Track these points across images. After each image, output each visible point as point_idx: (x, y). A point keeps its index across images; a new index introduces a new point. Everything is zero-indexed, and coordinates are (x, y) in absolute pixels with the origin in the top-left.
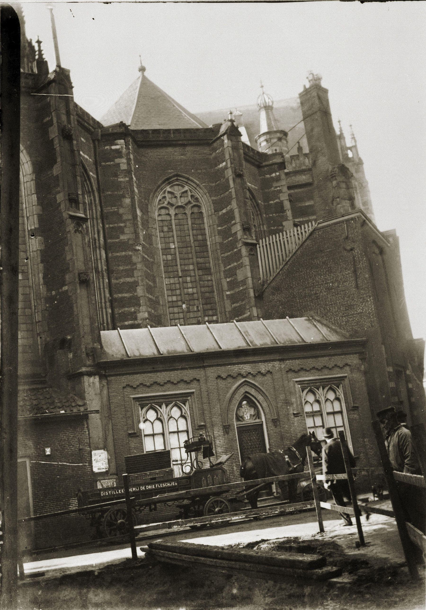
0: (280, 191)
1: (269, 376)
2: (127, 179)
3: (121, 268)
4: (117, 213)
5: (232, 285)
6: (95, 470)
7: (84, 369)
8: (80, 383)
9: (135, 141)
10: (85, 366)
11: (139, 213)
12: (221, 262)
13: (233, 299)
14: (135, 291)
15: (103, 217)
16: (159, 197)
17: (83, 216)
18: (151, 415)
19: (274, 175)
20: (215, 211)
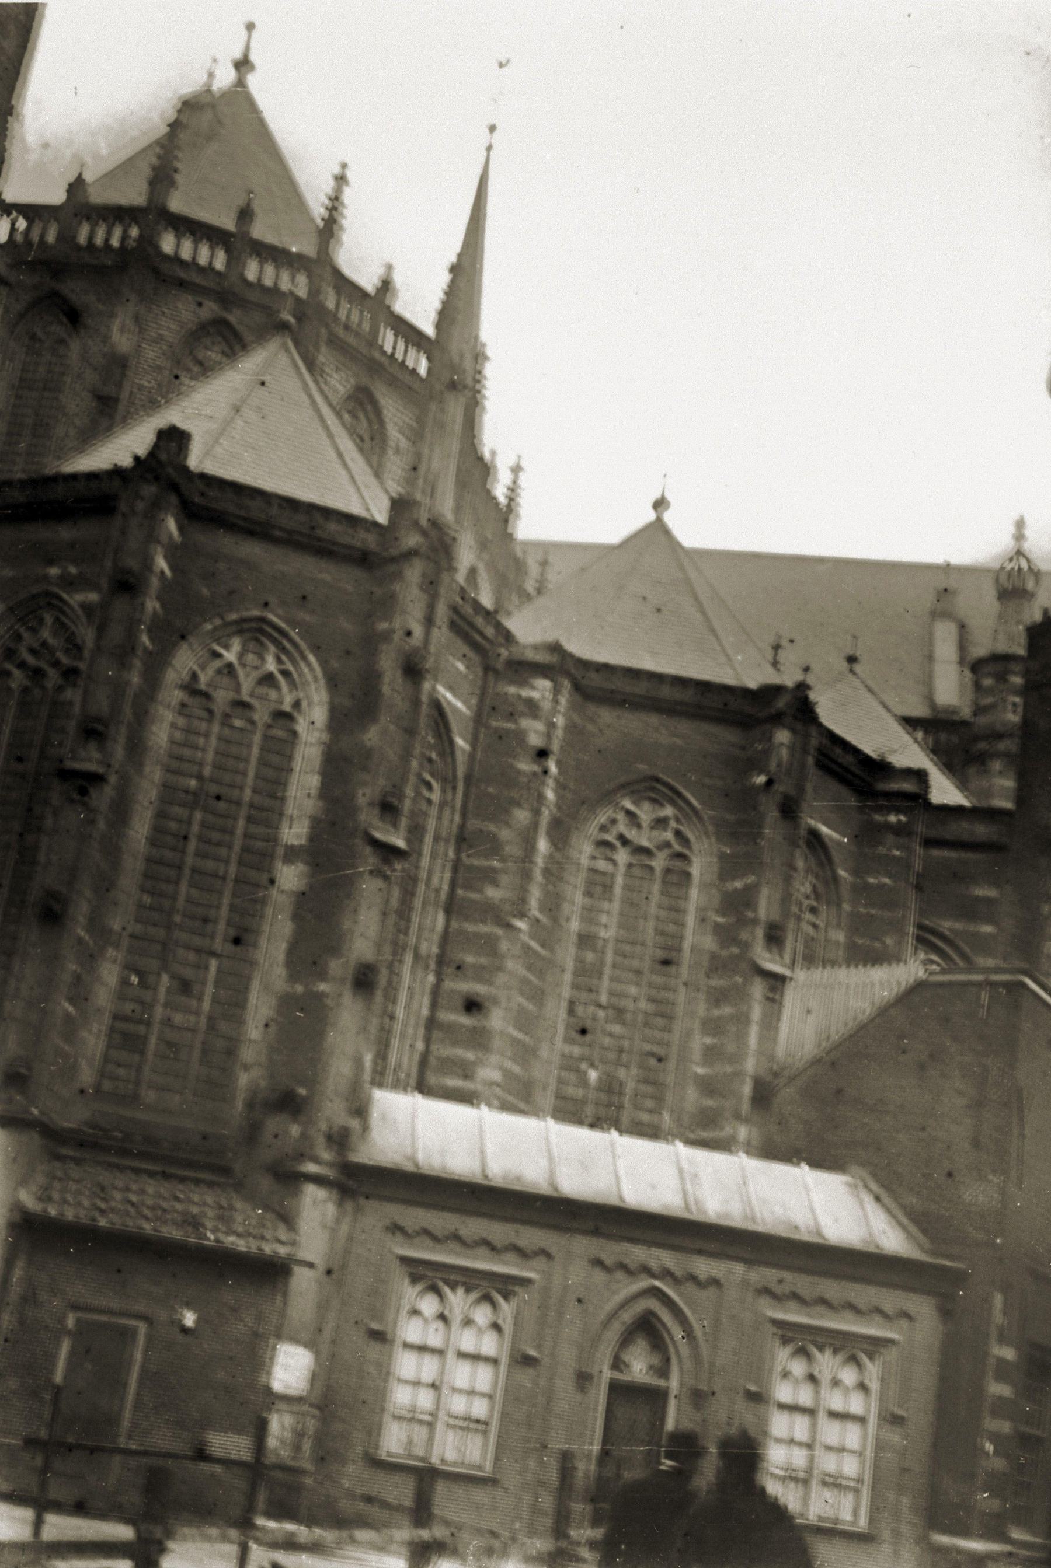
1: (712, 1292)
4: (493, 839)
5: (711, 1054)
6: (277, 1386)
7: (311, 1168)
8: (296, 1193)
9: (577, 687)
10: (316, 1160)
11: (543, 845)
13: (708, 1087)
15: (462, 840)
16: (603, 819)
17: (401, 843)
18: (429, 1305)
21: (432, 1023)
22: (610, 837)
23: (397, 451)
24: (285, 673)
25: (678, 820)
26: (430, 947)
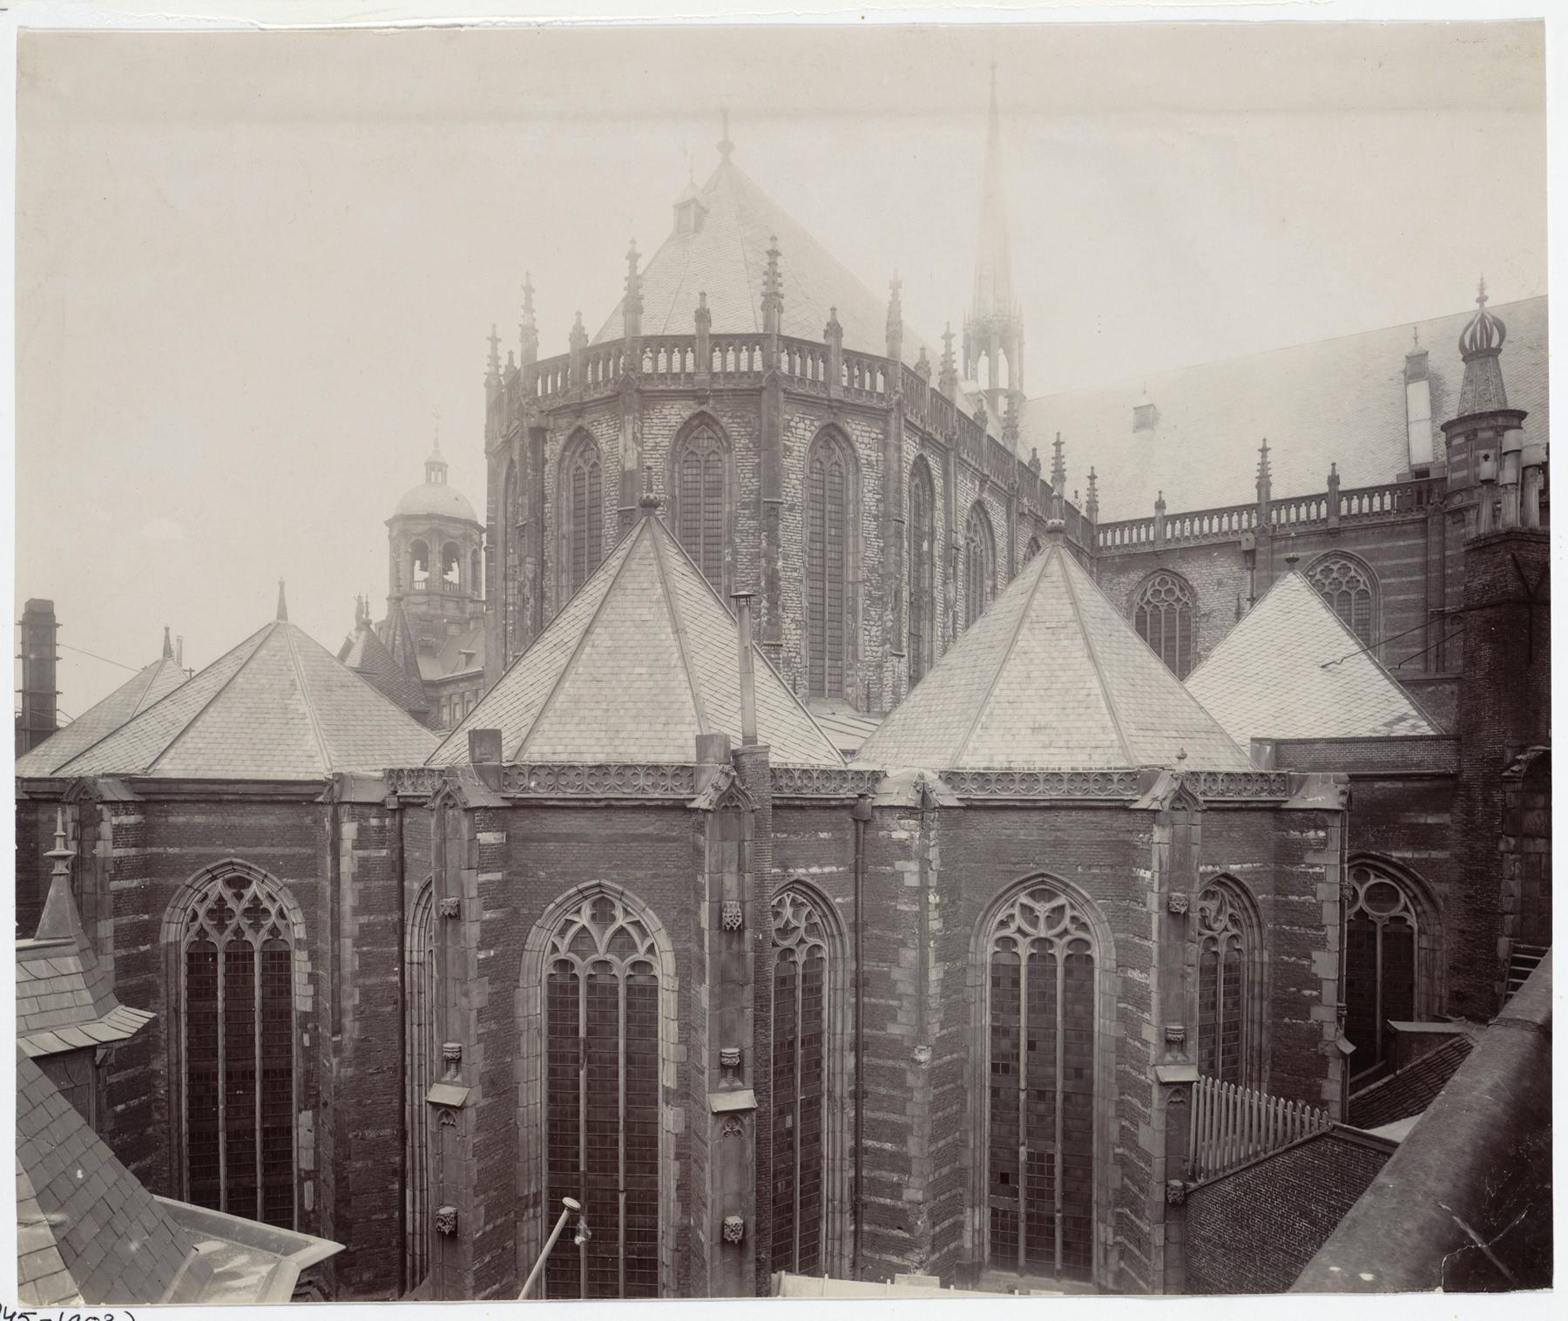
0: (1320, 878)
2: (916, 908)
3: (883, 1091)
4: (885, 976)
12: (1113, 1081)
14: (904, 1142)
16: (1001, 916)
19: (1311, 834)
20: (1118, 966)
21: (857, 1152)
22: (1008, 932)
23: (869, 464)
24: (637, 924)
25: (1073, 907)
26: (844, 1087)
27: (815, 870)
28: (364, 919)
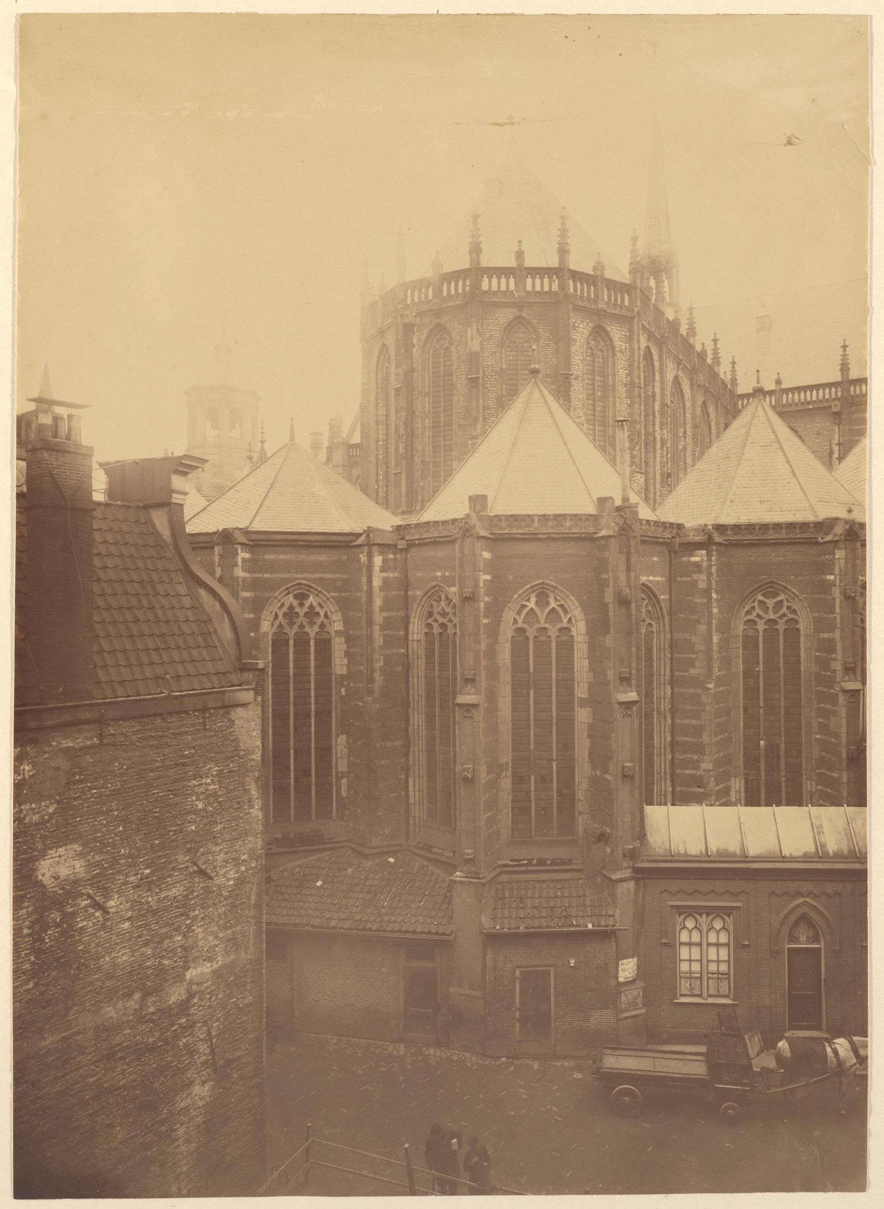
21: (673, 744)
25: (788, 601)
27: (651, 578)
28: (385, 614)
